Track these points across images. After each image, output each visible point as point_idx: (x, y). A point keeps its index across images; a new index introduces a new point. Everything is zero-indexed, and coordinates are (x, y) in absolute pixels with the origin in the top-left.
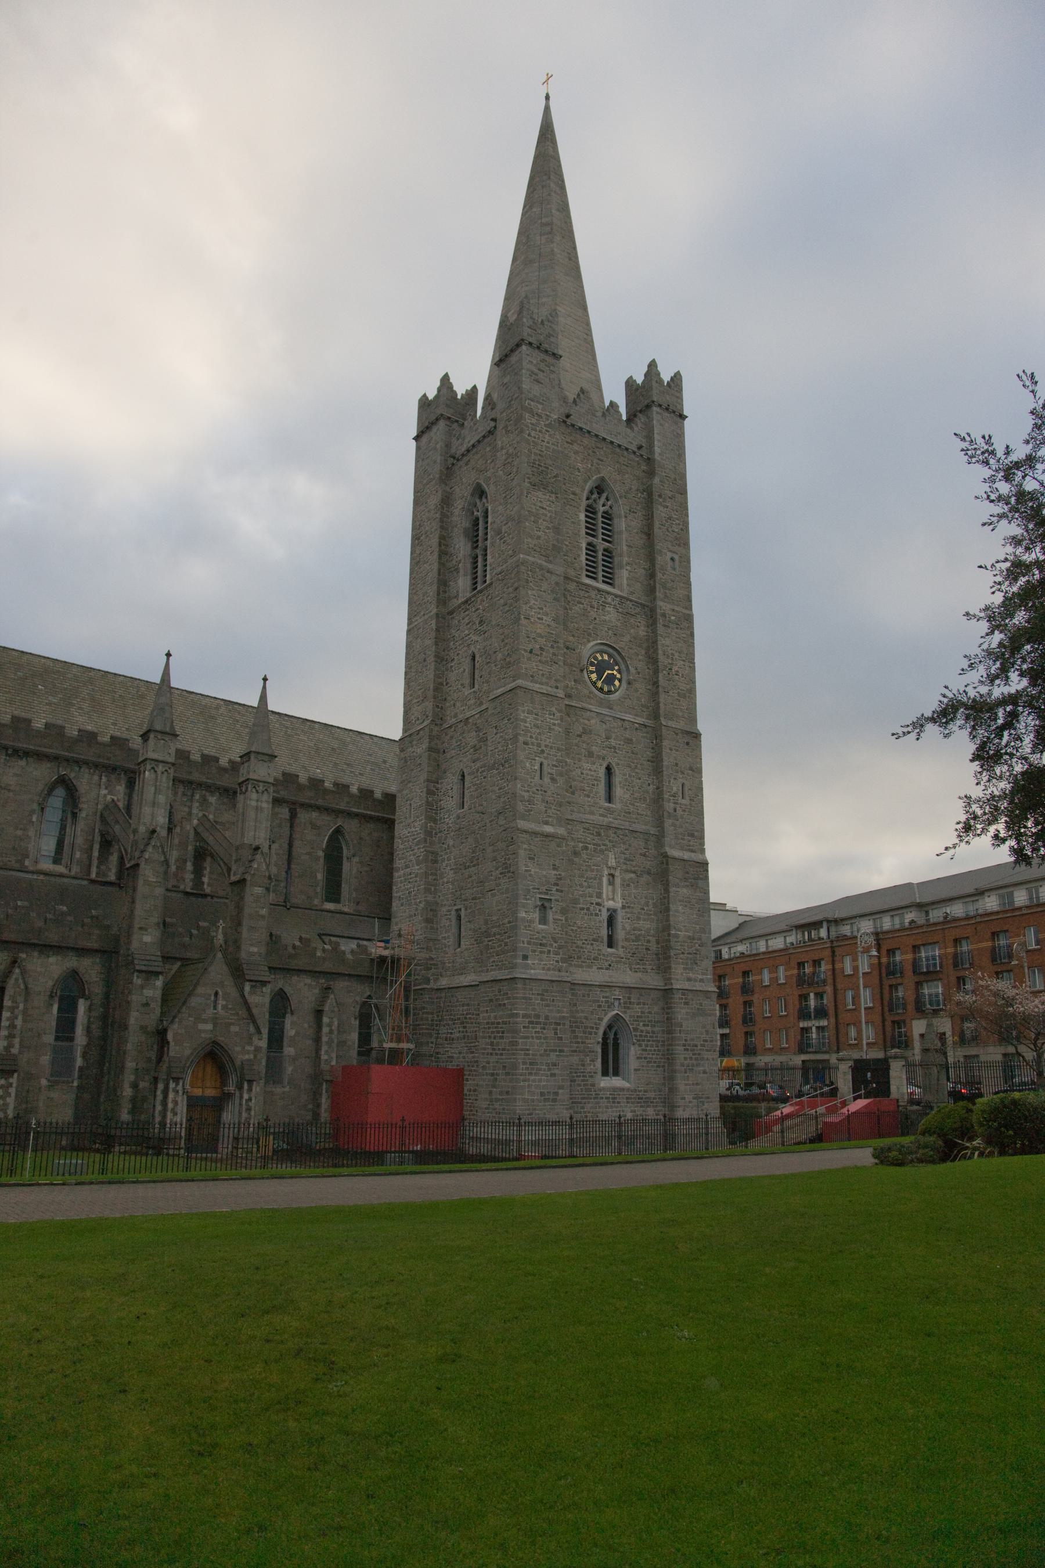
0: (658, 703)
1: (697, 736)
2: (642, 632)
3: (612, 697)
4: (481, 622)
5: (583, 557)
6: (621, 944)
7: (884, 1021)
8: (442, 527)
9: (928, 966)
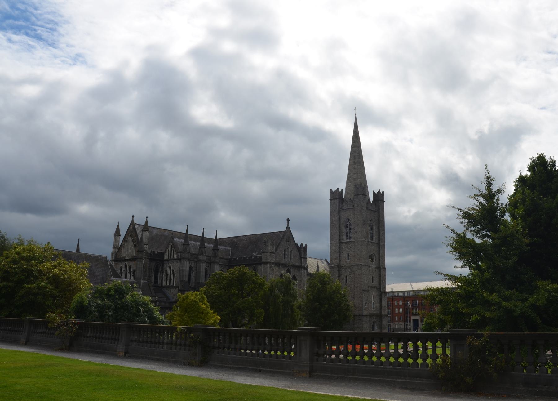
1: (385, 268)
3: (373, 263)
4: (350, 248)
5: (369, 236)
6: (375, 308)
7: (404, 316)
8: (339, 224)
9: (415, 305)
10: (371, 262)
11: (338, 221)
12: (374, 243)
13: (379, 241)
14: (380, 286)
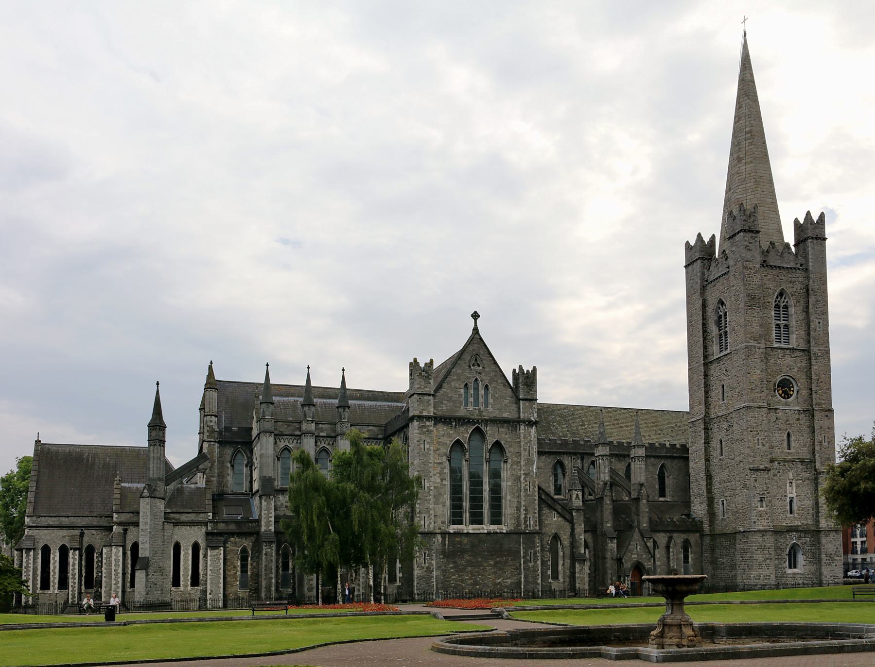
0: (812, 399)
2: (804, 364)
8: (704, 319)
10: (784, 398)
11: (701, 312)
12: (793, 350)
13: (809, 342)
14: (814, 456)
